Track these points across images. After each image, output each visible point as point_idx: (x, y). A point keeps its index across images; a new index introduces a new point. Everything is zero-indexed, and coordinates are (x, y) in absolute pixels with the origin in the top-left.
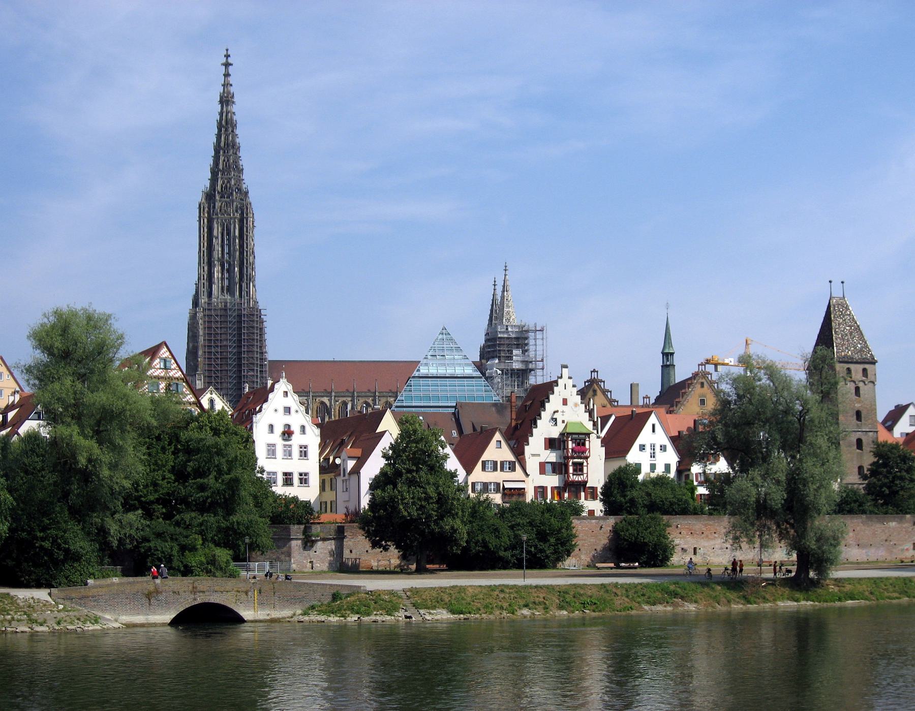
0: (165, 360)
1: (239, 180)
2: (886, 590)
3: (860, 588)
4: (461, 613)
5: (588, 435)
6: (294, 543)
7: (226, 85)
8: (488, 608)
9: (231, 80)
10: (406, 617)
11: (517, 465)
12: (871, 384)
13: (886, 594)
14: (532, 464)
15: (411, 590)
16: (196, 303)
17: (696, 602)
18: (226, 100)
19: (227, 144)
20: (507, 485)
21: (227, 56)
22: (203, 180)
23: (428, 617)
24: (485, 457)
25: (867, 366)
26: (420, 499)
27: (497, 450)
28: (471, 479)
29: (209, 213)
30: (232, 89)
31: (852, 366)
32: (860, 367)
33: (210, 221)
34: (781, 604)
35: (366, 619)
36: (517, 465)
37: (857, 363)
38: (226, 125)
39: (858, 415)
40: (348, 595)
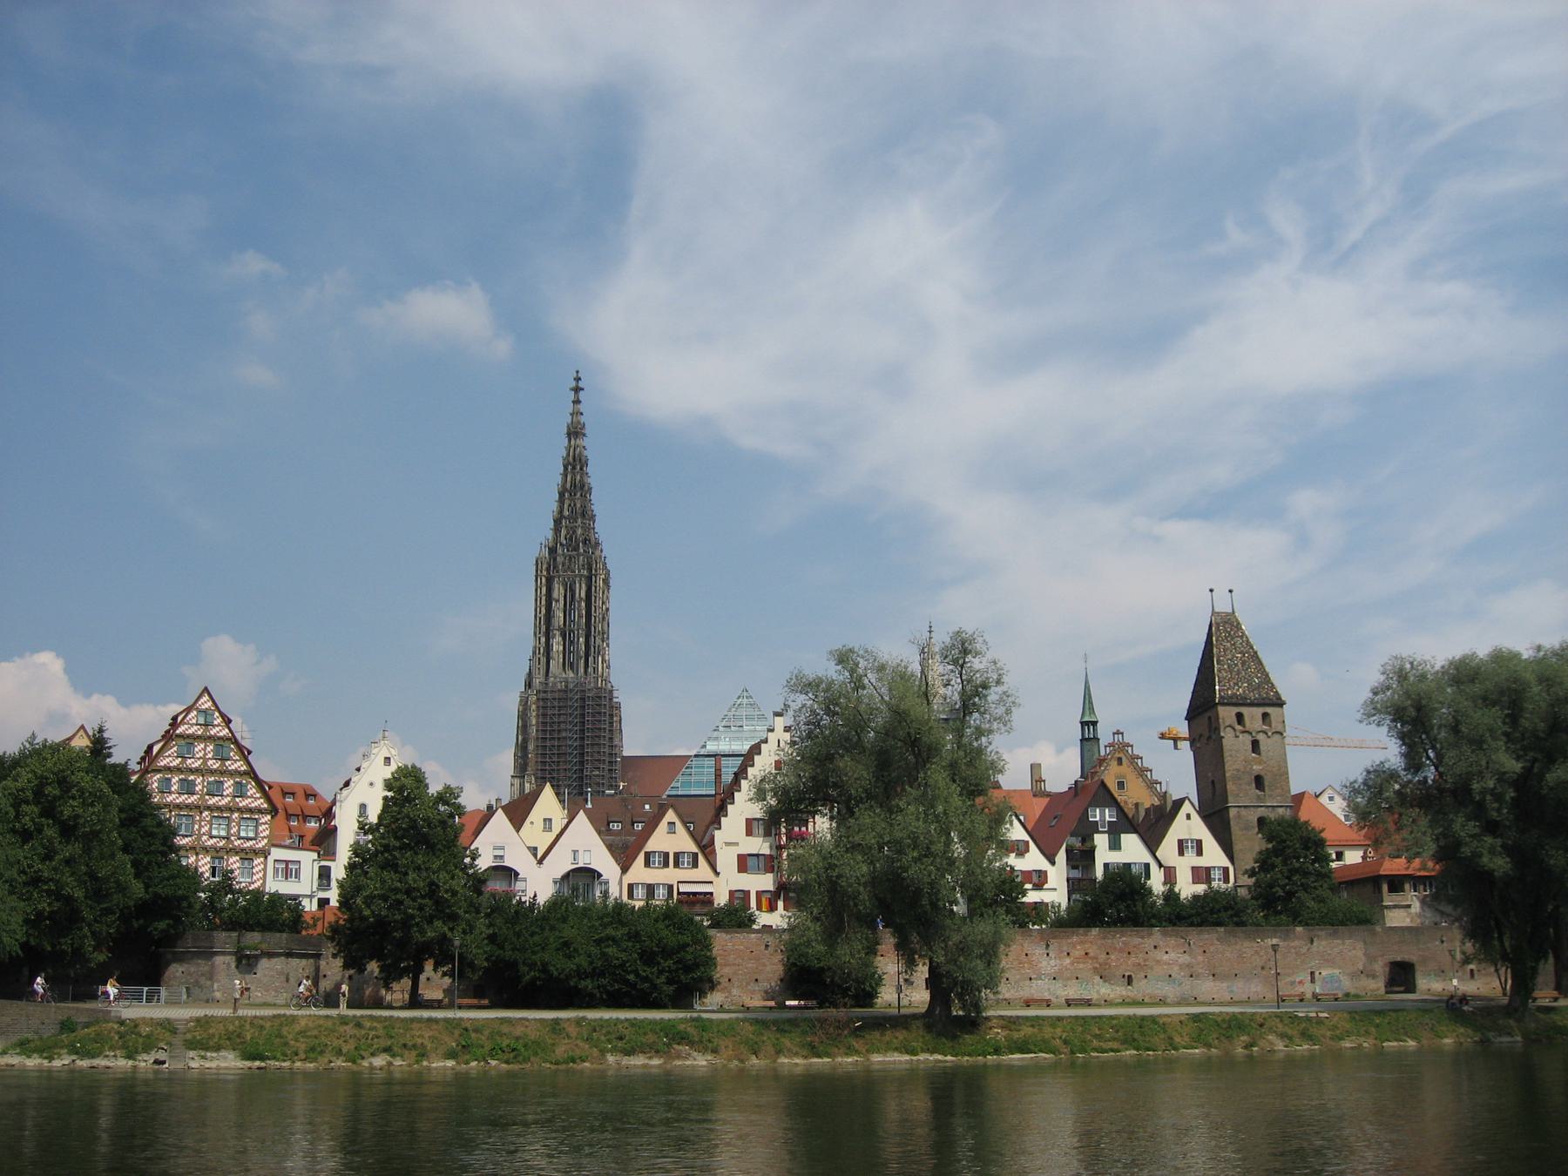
0: (205, 712)
1: (588, 529)
2: (1098, 1037)
3: (1048, 1032)
4: (253, 1058)
6: (219, 960)
8: (313, 1052)
10: (157, 1062)
11: (701, 858)
12: (1277, 737)
13: (1095, 1043)
14: (726, 858)
15: (198, 1020)
16: (529, 685)
17: (715, 1051)
18: (575, 432)
19: (574, 484)
20: (684, 888)
21: (578, 379)
22: (543, 530)
23: (193, 1064)
24: (651, 845)
25: (1269, 710)
26: (396, 891)
27: (670, 837)
28: (630, 877)
29: (548, 570)
30: (583, 419)
31: (1245, 710)
32: (1259, 711)
33: (550, 581)
34: (877, 1058)
35: (84, 1063)
36: (701, 858)
37: (1252, 705)
39: (1259, 781)
40: (87, 1025)
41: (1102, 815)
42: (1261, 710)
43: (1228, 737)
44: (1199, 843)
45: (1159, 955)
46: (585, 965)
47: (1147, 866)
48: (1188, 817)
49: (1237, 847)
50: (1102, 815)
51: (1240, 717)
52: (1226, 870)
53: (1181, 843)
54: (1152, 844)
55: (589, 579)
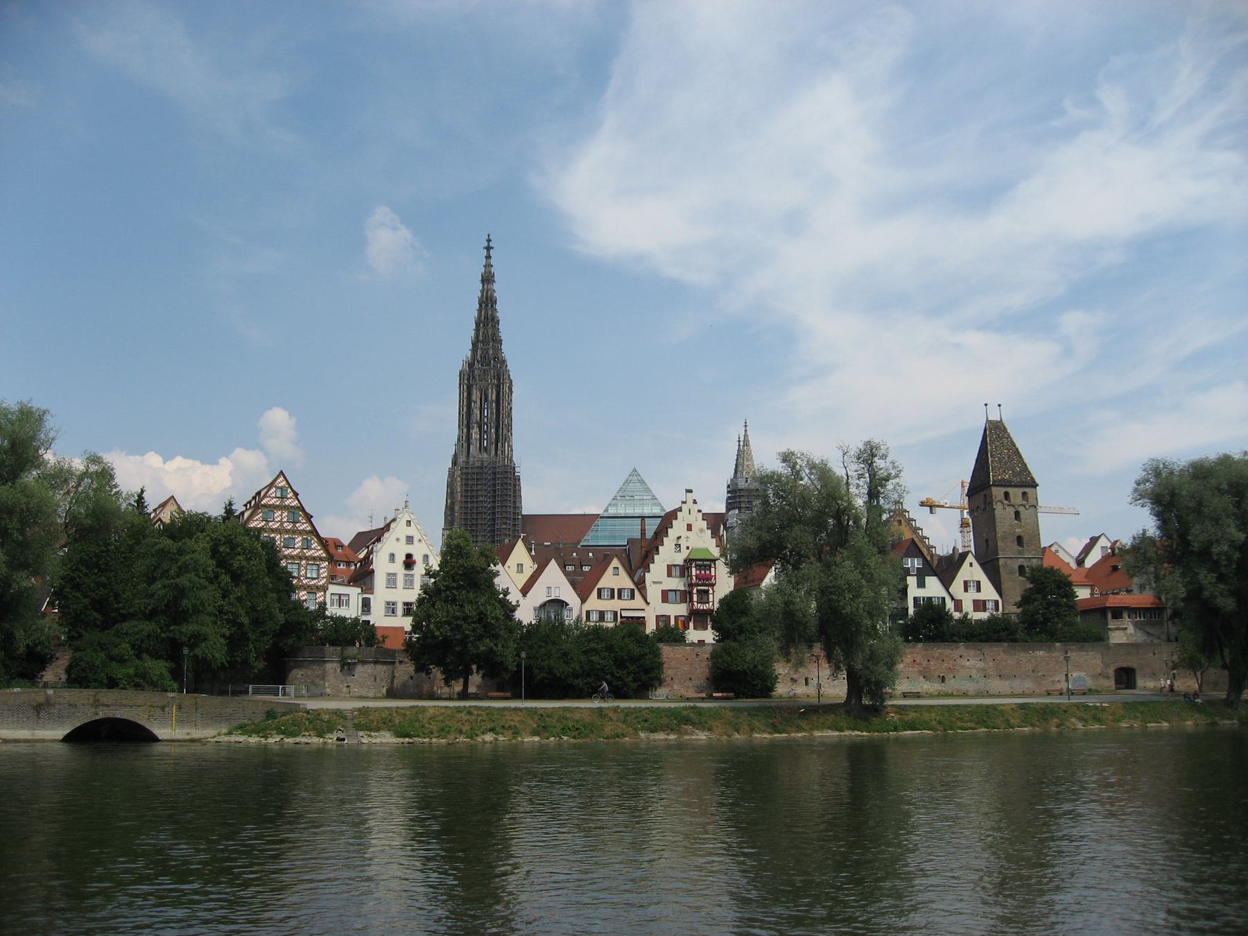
0: (281, 488)
1: (498, 350)
2: (960, 719)
3: (926, 716)
4: (405, 737)
5: (714, 561)
6: (329, 666)
7: (488, 266)
8: (443, 732)
9: (492, 261)
10: (338, 739)
11: (636, 592)
13: (959, 724)
14: (654, 593)
15: (359, 710)
16: (455, 463)
17: (710, 730)
18: (488, 279)
19: (486, 318)
20: (625, 614)
21: (489, 241)
22: (466, 351)
23: (364, 741)
24: (599, 585)
25: (1026, 490)
26: (457, 618)
27: (615, 577)
28: (586, 607)
30: (493, 270)
31: (1010, 490)
32: (1020, 491)
33: (469, 388)
34: (817, 734)
35: (290, 740)
36: (636, 592)
37: (1015, 486)
38: (487, 303)
39: (1020, 540)
40: (284, 714)
41: (913, 563)
42: (1022, 490)
43: (998, 509)
44: (978, 583)
45: (964, 662)
46: (578, 668)
47: (944, 599)
48: (971, 565)
49: (1004, 586)
50: (913, 563)
51: (1007, 495)
52: (996, 602)
53: (966, 583)
54: (946, 584)
55: (498, 386)
